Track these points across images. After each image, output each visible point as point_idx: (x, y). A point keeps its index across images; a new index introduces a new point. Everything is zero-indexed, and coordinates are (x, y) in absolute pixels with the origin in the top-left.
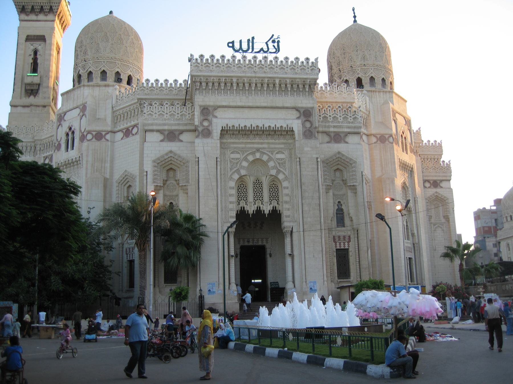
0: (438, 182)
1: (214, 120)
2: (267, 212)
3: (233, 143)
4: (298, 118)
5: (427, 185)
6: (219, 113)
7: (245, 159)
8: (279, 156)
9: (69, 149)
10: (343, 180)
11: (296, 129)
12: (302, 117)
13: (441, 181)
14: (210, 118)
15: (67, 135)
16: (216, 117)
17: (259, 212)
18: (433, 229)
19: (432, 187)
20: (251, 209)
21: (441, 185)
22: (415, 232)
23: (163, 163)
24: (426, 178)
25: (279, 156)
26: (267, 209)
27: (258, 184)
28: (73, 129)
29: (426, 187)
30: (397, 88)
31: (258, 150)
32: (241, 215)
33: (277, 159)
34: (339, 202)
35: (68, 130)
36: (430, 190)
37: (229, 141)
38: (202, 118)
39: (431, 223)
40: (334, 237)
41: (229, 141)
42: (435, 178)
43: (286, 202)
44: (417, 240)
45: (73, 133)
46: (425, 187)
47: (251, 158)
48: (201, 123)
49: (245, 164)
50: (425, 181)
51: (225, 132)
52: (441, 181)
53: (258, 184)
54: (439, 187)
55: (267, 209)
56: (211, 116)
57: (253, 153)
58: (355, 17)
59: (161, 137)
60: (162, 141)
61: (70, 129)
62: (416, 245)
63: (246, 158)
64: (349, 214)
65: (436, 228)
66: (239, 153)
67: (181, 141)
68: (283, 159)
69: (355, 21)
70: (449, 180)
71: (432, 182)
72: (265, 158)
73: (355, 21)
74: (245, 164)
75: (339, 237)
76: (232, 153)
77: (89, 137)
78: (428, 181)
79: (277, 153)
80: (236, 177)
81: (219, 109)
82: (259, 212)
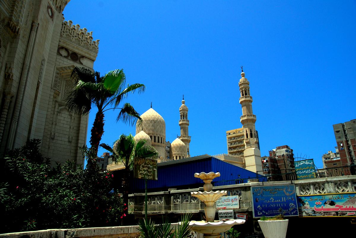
0: (79, 56)
5: (64, 53)
13: (83, 57)
18: (56, 110)
19: (69, 58)
21: (82, 61)
22: (15, 73)
24: (65, 45)
29: (61, 55)
36: (65, 60)
39: (56, 101)
42: (76, 51)
44: (14, 90)
46: (59, 53)
50: (61, 48)
52: (83, 57)
54: (78, 61)
62: (9, 97)
65: (61, 110)
70: (93, 61)
71: (70, 52)
78: (67, 50)
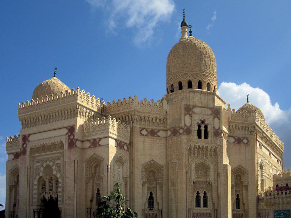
1: (28, 143)
3: (38, 156)
6: (31, 138)
7: (42, 166)
14: (26, 142)
17: (51, 198)
20: (47, 197)
23: (14, 172)
27: (51, 180)
31: (48, 159)
32: (44, 200)
33: (57, 164)
34: (98, 189)
37: (36, 155)
38: (23, 142)
40: (94, 213)
41: (36, 155)
47: (45, 165)
48: (23, 145)
49: (42, 169)
51: (32, 150)
55: (54, 196)
56: (27, 141)
57: (46, 161)
60: (13, 159)
63: (43, 165)
66: (39, 162)
68: (60, 163)
72: (51, 164)
76: (37, 163)
79: (57, 160)
80: (38, 177)
81: (31, 136)
82: (51, 198)
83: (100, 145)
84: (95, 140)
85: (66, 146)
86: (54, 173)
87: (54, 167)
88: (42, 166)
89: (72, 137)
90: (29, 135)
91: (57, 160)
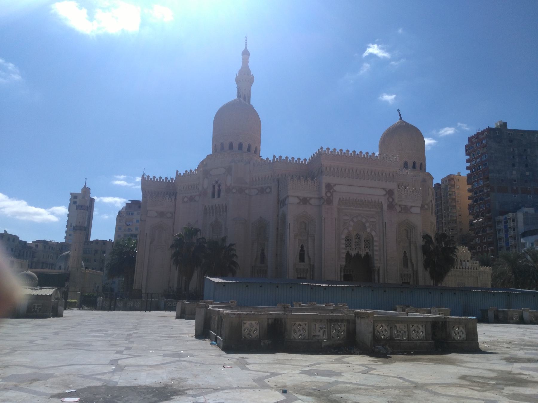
2: (363, 256)
4: (384, 195)
7: (352, 220)
8: (372, 220)
9: (216, 197)
10: (407, 237)
11: (383, 203)
12: (387, 195)
14: (331, 191)
15: (214, 186)
16: (335, 191)
17: (358, 255)
20: (353, 253)
25: (372, 220)
26: (363, 253)
28: (219, 182)
30: (428, 170)
35: (214, 183)
38: (327, 191)
43: (376, 251)
45: (219, 186)
48: (326, 194)
53: (358, 236)
58: (400, 115)
59: (298, 201)
61: (217, 182)
64: (411, 260)
67: (311, 204)
69: (401, 119)
73: (401, 119)
74: (352, 223)
75: (404, 275)
77: (234, 191)
80: (346, 231)
82: (358, 255)
83: (411, 213)
84: (406, 207)
85: (385, 207)
86: (368, 230)
87: (367, 225)
88: (352, 220)
89: (391, 200)
90: (335, 185)
91: (372, 218)
